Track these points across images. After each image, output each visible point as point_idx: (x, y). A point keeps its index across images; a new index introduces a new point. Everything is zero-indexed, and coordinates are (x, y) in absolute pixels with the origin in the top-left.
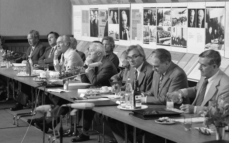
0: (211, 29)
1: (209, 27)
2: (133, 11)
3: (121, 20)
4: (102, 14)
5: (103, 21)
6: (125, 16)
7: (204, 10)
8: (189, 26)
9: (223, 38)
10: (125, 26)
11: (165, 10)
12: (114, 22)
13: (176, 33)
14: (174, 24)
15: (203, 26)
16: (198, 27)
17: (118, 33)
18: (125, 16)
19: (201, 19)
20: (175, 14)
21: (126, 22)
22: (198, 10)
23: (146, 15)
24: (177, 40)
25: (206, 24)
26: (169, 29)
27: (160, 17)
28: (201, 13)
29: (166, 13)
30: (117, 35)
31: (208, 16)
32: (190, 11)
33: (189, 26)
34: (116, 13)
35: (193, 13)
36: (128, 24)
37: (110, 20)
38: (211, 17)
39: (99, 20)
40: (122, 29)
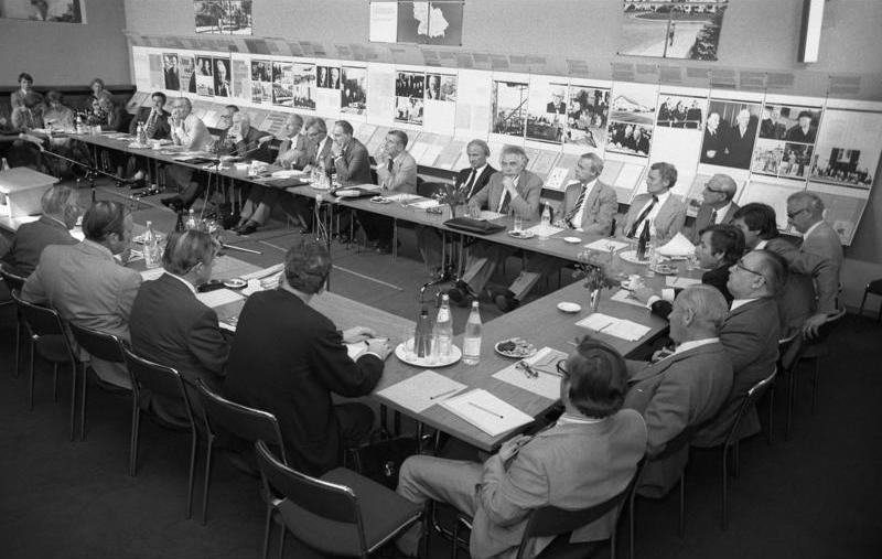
0: (348, 92)
1: (345, 89)
2: (235, 62)
3: (217, 71)
4: (185, 62)
5: (187, 70)
6: (222, 67)
8: (319, 85)
10: (223, 80)
11: (283, 65)
12: (205, 73)
13: (301, 91)
14: (297, 82)
15: (338, 87)
16: (331, 87)
17: (212, 87)
18: (222, 67)
19: (335, 79)
20: (298, 70)
21: (224, 75)
22: (330, 68)
23: (255, 68)
25: (342, 85)
26: (290, 88)
27: (277, 73)
28: (335, 72)
29: (286, 68)
30: (210, 90)
31: (344, 77)
33: (319, 85)
34: (207, 63)
35: (324, 71)
36: (228, 77)
37: (197, 69)
38: (348, 78)
39: (181, 69)
40: (217, 82)
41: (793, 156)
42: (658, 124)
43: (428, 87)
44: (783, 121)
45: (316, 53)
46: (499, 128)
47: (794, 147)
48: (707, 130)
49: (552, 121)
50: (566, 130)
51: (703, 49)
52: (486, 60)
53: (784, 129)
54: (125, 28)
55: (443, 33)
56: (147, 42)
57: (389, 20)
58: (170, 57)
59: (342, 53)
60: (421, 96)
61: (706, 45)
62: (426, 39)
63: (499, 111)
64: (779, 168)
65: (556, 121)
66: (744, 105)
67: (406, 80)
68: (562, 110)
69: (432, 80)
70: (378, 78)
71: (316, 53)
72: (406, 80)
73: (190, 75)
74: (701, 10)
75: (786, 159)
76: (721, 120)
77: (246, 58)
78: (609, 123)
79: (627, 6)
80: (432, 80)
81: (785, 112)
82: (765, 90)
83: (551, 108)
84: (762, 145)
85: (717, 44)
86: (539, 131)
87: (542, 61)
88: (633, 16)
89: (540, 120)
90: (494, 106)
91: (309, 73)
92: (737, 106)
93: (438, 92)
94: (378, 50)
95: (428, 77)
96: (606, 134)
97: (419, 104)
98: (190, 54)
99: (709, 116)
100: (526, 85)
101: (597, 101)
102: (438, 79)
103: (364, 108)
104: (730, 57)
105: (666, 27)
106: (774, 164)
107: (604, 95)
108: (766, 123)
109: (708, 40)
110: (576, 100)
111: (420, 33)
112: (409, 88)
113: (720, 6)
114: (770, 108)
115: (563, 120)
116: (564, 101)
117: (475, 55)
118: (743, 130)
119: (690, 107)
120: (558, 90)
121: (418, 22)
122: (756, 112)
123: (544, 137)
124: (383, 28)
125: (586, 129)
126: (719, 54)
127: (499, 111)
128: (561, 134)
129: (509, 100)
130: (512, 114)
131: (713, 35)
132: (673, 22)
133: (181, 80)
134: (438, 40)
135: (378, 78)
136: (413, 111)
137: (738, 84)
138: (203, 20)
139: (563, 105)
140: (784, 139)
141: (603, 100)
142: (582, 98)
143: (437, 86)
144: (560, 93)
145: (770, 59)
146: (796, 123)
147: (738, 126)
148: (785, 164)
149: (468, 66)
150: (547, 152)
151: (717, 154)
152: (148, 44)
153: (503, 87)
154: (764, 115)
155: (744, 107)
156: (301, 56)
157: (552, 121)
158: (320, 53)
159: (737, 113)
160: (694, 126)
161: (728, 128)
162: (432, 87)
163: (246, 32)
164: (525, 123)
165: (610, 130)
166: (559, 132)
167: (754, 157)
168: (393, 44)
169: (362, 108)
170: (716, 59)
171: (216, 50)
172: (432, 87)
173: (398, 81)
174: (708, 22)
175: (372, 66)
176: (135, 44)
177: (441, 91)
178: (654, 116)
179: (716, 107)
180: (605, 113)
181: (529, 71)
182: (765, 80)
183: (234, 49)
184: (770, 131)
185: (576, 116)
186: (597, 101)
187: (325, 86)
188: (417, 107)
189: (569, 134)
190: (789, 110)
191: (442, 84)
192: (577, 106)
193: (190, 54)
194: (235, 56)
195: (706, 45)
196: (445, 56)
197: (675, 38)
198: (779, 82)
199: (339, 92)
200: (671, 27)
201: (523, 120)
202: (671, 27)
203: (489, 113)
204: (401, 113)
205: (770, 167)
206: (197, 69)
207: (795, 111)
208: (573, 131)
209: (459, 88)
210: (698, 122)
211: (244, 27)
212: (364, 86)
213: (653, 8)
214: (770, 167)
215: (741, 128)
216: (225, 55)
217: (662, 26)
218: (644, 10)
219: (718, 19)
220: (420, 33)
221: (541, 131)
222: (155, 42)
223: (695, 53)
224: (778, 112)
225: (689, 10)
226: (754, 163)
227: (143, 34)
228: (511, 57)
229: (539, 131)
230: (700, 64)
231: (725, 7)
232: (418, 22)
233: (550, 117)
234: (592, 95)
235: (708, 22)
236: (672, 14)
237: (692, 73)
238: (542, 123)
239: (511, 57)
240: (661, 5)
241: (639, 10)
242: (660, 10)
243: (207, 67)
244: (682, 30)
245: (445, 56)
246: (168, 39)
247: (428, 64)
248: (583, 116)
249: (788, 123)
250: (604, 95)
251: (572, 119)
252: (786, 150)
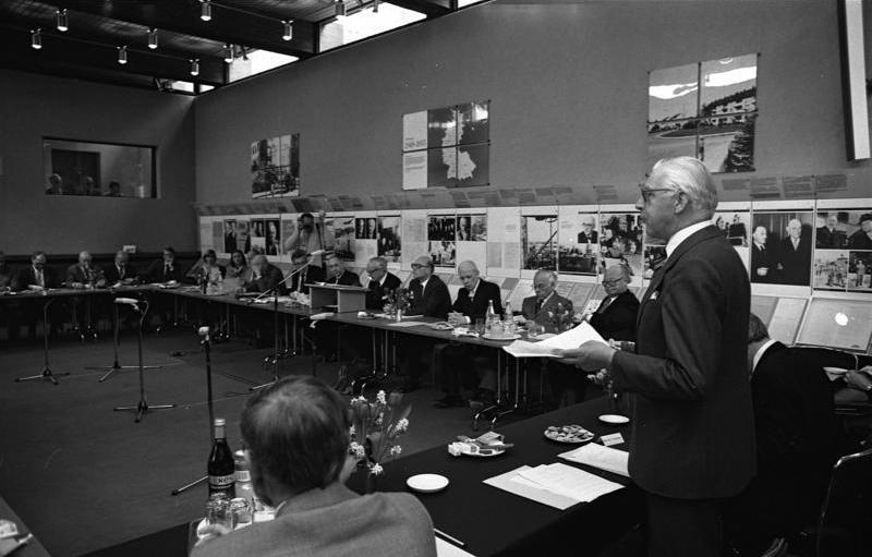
0: (384, 241)
1: (382, 238)
2: (284, 221)
4: (242, 226)
5: (244, 234)
6: (273, 228)
7: (375, 219)
9: (399, 249)
10: (274, 240)
12: (258, 235)
14: (338, 235)
15: (374, 237)
16: (368, 238)
17: (264, 247)
18: (273, 228)
19: (372, 229)
20: (339, 225)
21: (274, 235)
22: (368, 219)
24: (695, 127)
25: (378, 235)
28: (372, 223)
30: (262, 249)
31: (380, 226)
32: (358, 220)
33: (357, 237)
35: (362, 223)
36: (278, 237)
37: (252, 232)
39: (238, 233)
40: (269, 242)
41: (861, 266)
43: (459, 228)
44: (842, 227)
45: (355, 206)
46: (530, 264)
47: (859, 255)
48: (754, 247)
49: (584, 252)
50: (599, 259)
51: (738, 160)
52: (513, 195)
53: (845, 237)
54: (195, 200)
55: (471, 175)
56: (211, 211)
57: (421, 168)
58: (230, 223)
59: (378, 205)
60: (453, 238)
61: (740, 156)
62: (456, 183)
63: (529, 246)
64: (846, 281)
65: (588, 251)
66: (793, 214)
68: (594, 241)
69: (463, 221)
70: (410, 223)
71: (355, 206)
72: (438, 224)
73: (245, 238)
74: (729, 121)
75: (853, 269)
76: (768, 233)
77: (294, 217)
78: (644, 248)
79: (651, 127)
80: (463, 221)
81: (843, 216)
82: (815, 196)
83: (582, 238)
84: (820, 256)
85: (752, 154)
86: (573, 263)
87: (569, 190)
88: (658, 136)
89: (572, 252)
90: (524, 241)
91: (349, 226)
92: (786, 216)
93: (468, 232)
94: (411, 197)
95: (459, 219)
96: (643, 260)
97: (451, 246)
98: (246, 218)
99: (754, 230)
100: (555, 217)
101: (629, 226)
102: (468, 218)
103: (399, 255)
104: (770, 163)
105: (694, 143)
106: (839, 276)
107: (636, 219)
108: (822, 232)
109: (742, 151)
110: (607, 227)
111: (449, 177)
112: (441, 231)
113: (750, 115)
114: (823, 214)
115: (596, 248)
116: (596, 229)
117: (502, 191)
118: (796, 242)
119: (731, 223)
120: (587, 219)
121: (447, 167)
122: (807, 221)
123: (575, 270)
124: (416, 177)
125: (620, 257)
126: (756, 165)
127: (529, 246)
128: (595, 264)
129: (539, 233)
130: (542, 248)
131: (746, 145)
132: (701, 137)
133: (238, 242)
134: (466, 183)
135: (410, 223)
136: (446, 254)
137: (782, 191)
138: (257, 188)
139: (595, 234)
140: (845, 248)
141: (636, 224)
142: (613, 224)
143: (468, 226)
144: (590, 222)
145: (813, 162)
146: (859, 228)
147: (789, 238)
148: (853, 276)
149: (497, 204)
150: (580, 285)
151: (768, 272)
152: (213, 214)
153: (531, 221)
154: (819, 223)
155: (793, 217)
156: (342, 210)
157: (584, 252)
158: (359, 206)
159: (786, 224)
161: (777, 241)
162: (463, 228)
163: (294, 193)
164: (557, 256)
165: (647, 256)
166: (593, 263)
167: (813, 270)
168: (424, 190)
169: (397, 255)
170: (754, 170)
171: (266, 212)
172: (463, 228)
173: (430, 225)
174: (739, 133)
175: (407, 214)
176: (203, 215)
177: (474, 231)
179: (760, 219)
180: (639, 238)
181: (558, 203)
182: (812, 184)
183: (283, 210)
184: (828, 239)
185: (609, 243)
186: (629, 226)
187: (363, 238)
188: (449, 250)
189: (603, 263)
190: (847, 214)
191: (472, 223)
192: (609, 234)
193: (246, 218)
194: (284, 217)
195: (740, 156)
196: (472, 196)
197: (706, 153)
198: (827, 186)
199: (375, 241)
200: (700, 142)
201: (555, 253)
202: (700, 142)
203: (520, 251)
204: (434, 257)
205: (835, 280)
206: (252, 232)
207: (855, 216)
208: (607, 260)
210: (742, 238)
211: (292, 190)
212: (400, 233)
213: (679, 125)
214: (835, 280)
215: (793, 240)
216: (276, 216)
217: (691, 142)
218: (669, 129)
219: (750, 128)
220: (449, 177)
221: (575, 264)
222: (258, 209)
223: (729, 165)
224: (835, 218)
225: (717, 123)
226: (814, 277)
227: (208, 204)
228: (537, 190)
229: (573, 263)
230: (735, 176)
231: (756, 116)
232: (447, 167)
233: (582, 247)
234: (623, 220)
235: (739, 133)
236: (699, 129)
237: (728, 186)
238: (574, 255)
239: (537, 190)
240: (686, 122)
241: (663, 130)
242: (686, 127)
243: (260, 228)
244: (711, 144)
245: (472, 196)
246: (228, 207)
247: (336, 210)
248: (617, 244)
249: (848, 230)
250: (636, 219)
251: (605, 248)
252: (851, 259)
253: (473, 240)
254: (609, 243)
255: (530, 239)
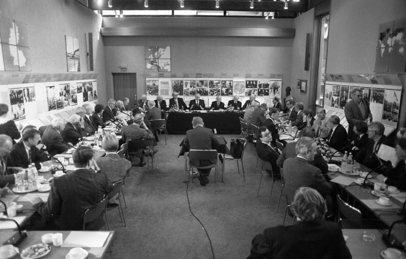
42: (78, 93)
43: (25, 96)
60: (22, 102)
67: (15, 94)
69: (26, 91)
80: (26, 91)
83: (61, 95)
93: (29, 97)
95: (24, 90)
97: (23, 107)
100: (54, 87)
136: (20, 112)
160: (81, 91)
172: (26, 95)
173: (11, 95)
178: (76, 91)
191: (30, 93)
204: (15, 115)
209: (36, 93)
233: (60, 98)
253: (31, 101)
254: (65, 96)
255: (49, 98)
